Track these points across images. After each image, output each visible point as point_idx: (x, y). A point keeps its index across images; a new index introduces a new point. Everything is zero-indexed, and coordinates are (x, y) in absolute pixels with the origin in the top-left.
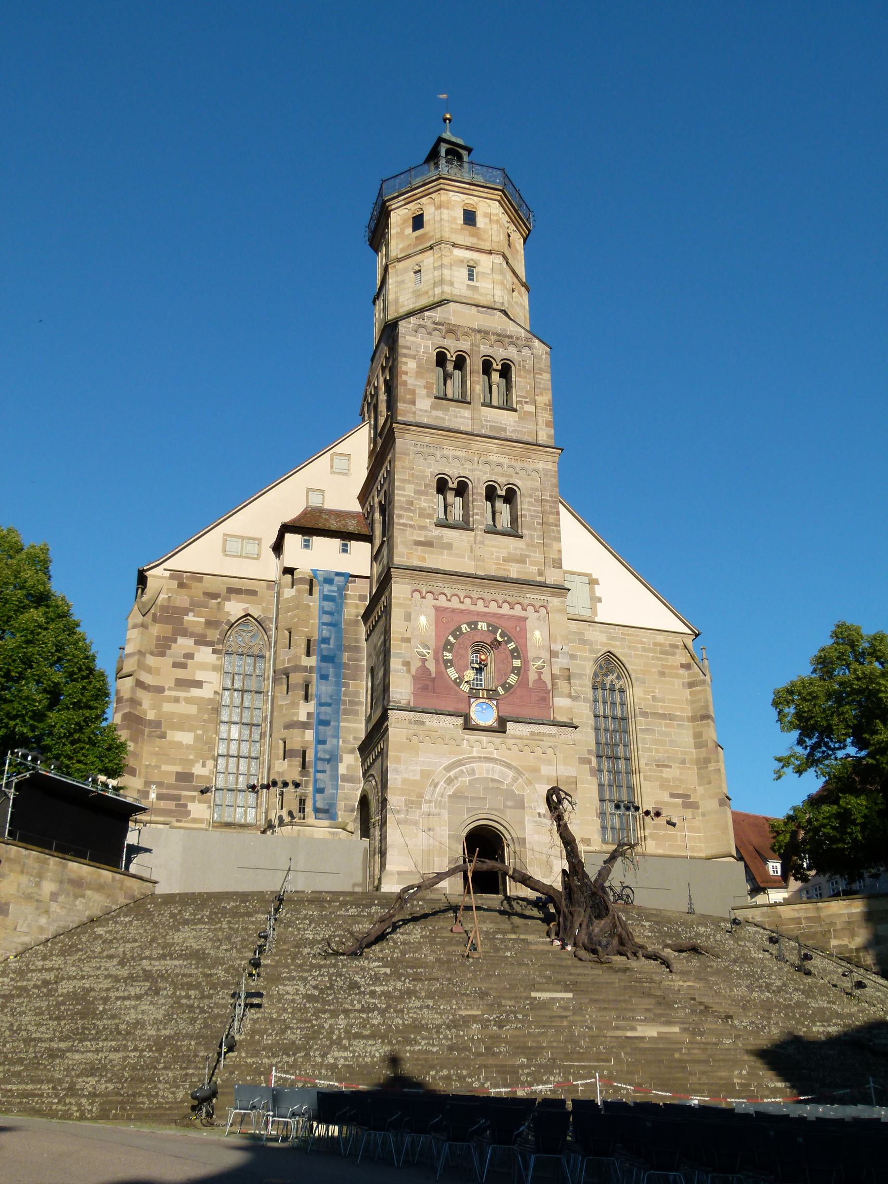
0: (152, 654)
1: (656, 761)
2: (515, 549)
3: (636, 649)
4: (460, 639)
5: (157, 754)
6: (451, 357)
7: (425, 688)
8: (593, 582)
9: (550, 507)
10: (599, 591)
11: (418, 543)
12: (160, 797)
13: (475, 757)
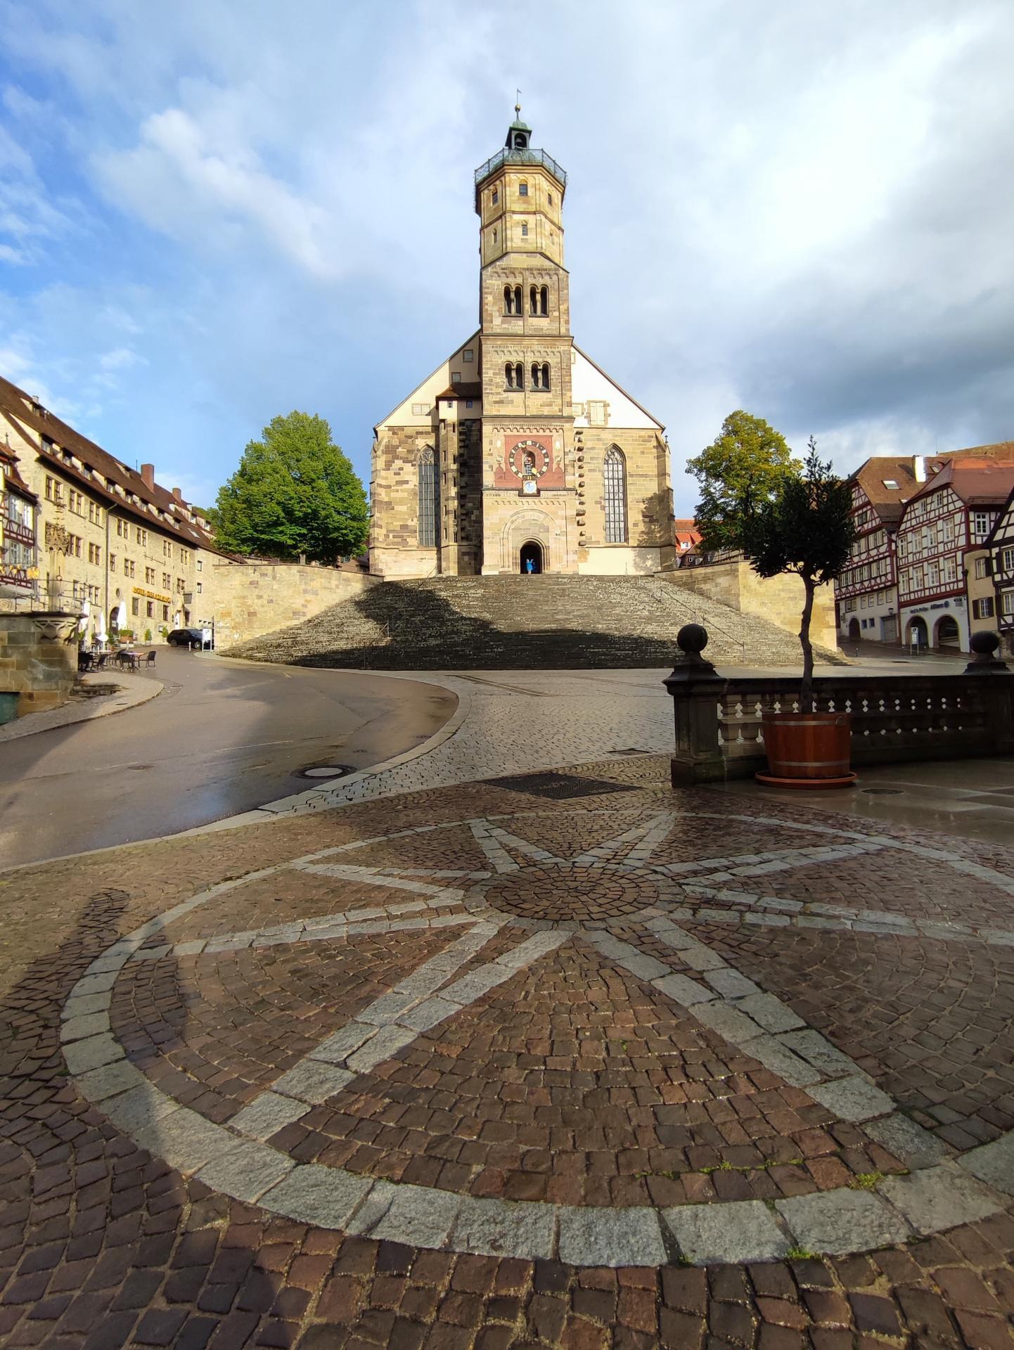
8: (606, 405)
10: (609, 410)
11: (496, 402)
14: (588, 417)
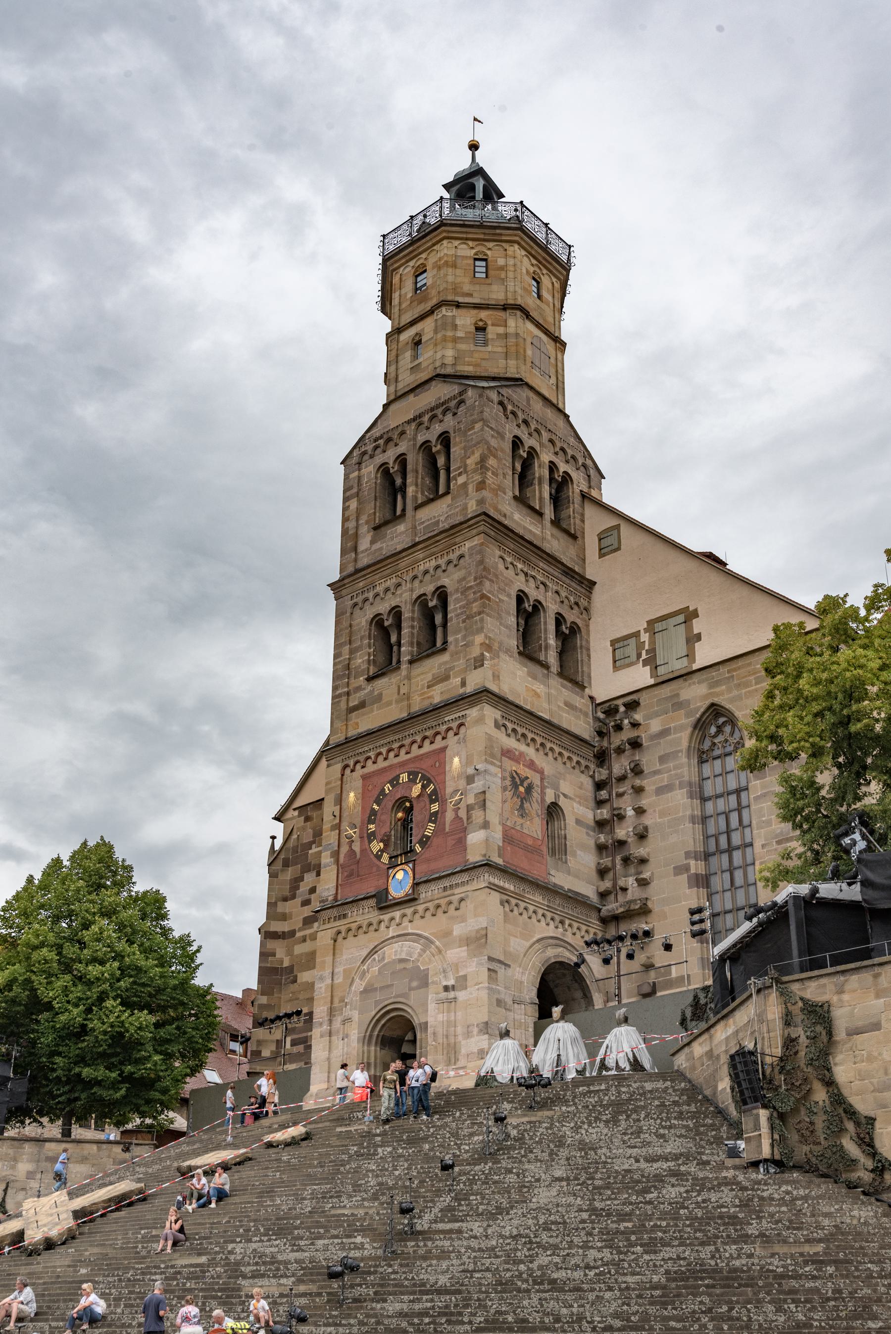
0: (285, 899)
1: (777, 836)
2: (440, 665)
3: (747, 684)
4: (383, 804)
5: (290, 1000)
6: (394, 468)
7: (350, 875)
8: (690, 615)
9: (474, 593)
10: (697, 626)
12: (294, 1043)
13: (393, 937)
14: (651, 662)
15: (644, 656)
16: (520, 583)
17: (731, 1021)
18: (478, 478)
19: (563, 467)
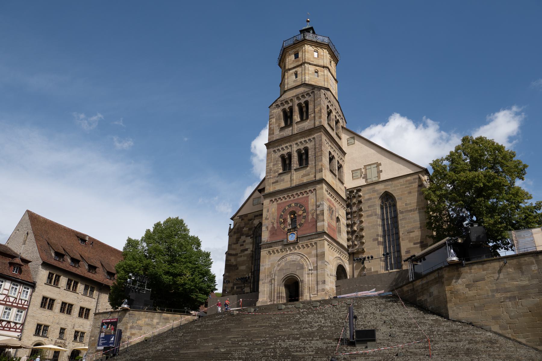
0: (234, 244)
7: (273, 234)
8: (378, 165)
10: (381, 168)
11: (273, 183)
12: (237, 288)
14: (365, 177)
15: (363, 176)
16: (329, 149)
17: (425, 279)
18: (319, 115)
19: (338, 118)
